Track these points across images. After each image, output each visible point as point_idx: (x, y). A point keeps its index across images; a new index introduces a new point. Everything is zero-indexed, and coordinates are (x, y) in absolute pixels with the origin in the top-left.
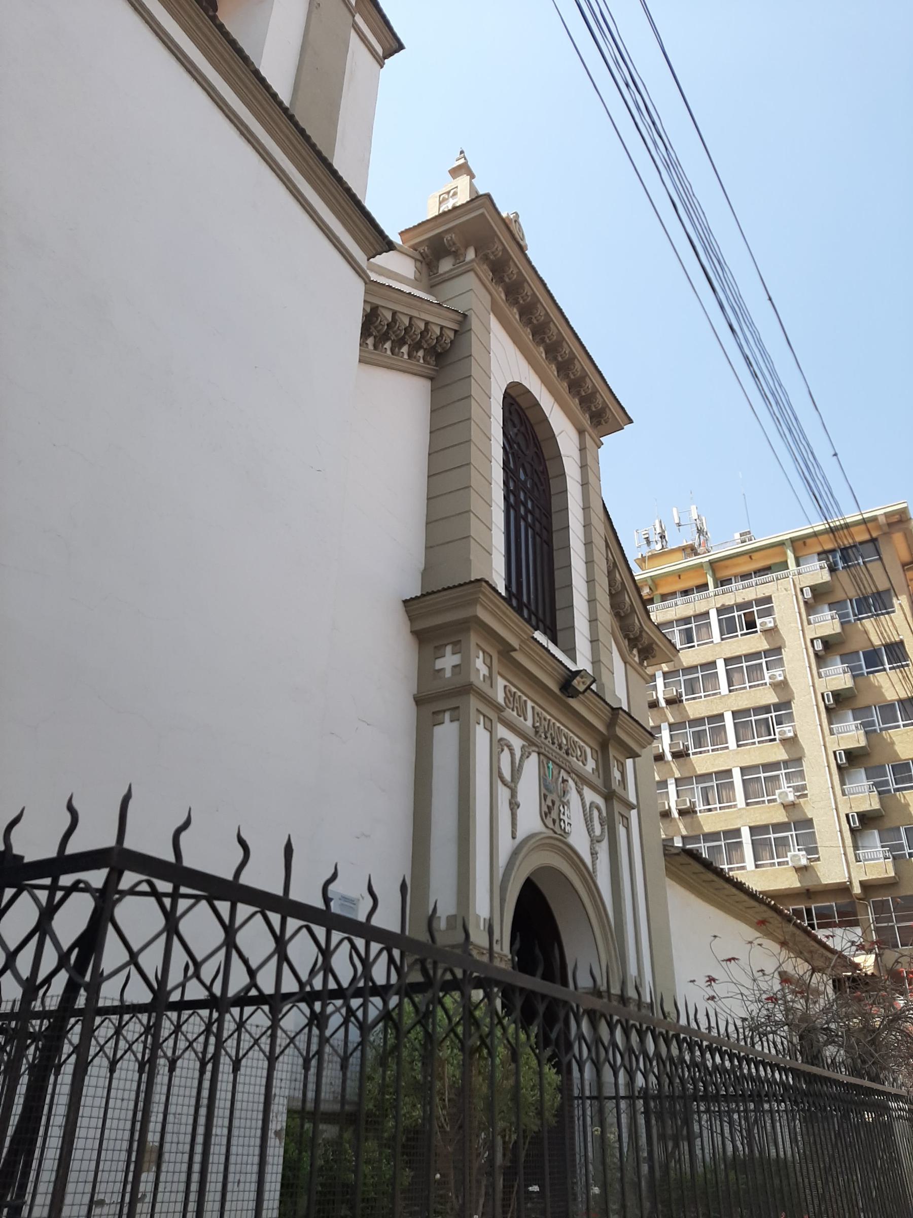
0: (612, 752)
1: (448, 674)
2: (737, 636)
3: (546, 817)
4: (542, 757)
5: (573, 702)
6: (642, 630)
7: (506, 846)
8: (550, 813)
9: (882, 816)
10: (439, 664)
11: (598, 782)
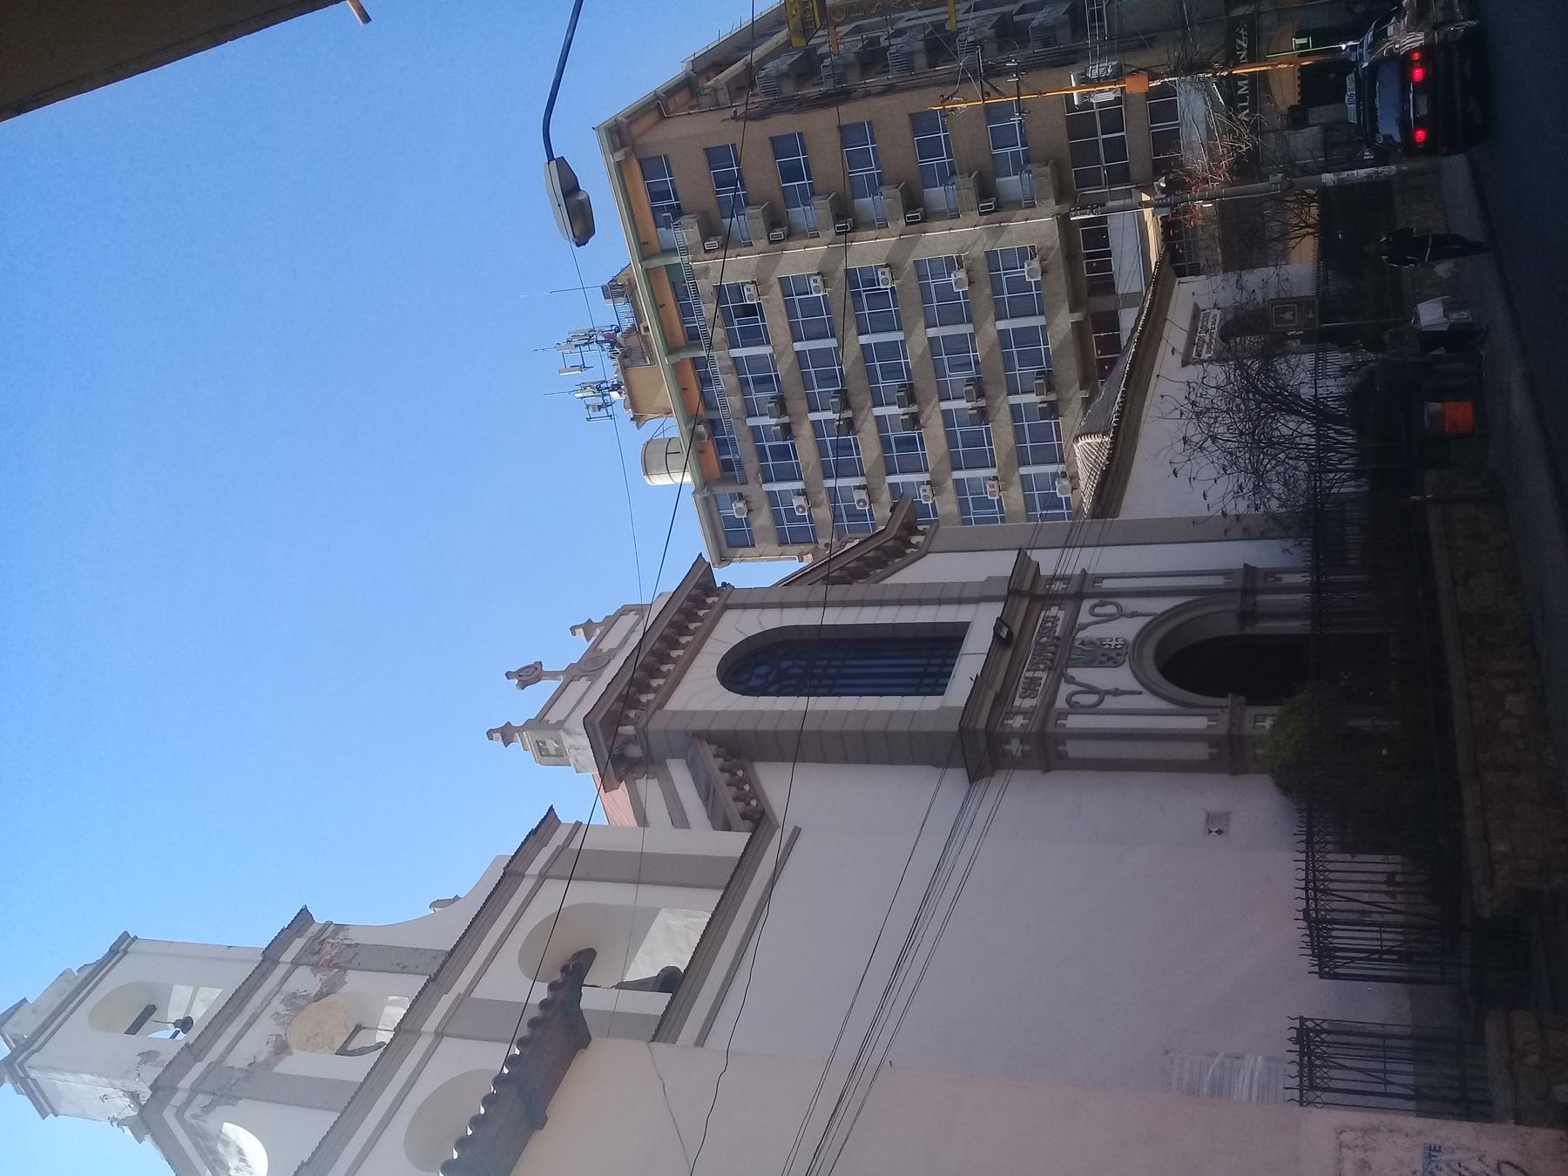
0: (1040, 591)
1: (1027, 748)
2: (764, 326)
3: (1115, 662)
4: (1069, 665)
5: (1016, 632)
6: (895, 538)
7: (1148, 701)
8: (1113, 658)
9: (980, 174)
10: (1019, 754)
11: (1070, 605)
